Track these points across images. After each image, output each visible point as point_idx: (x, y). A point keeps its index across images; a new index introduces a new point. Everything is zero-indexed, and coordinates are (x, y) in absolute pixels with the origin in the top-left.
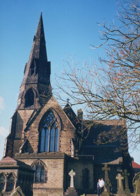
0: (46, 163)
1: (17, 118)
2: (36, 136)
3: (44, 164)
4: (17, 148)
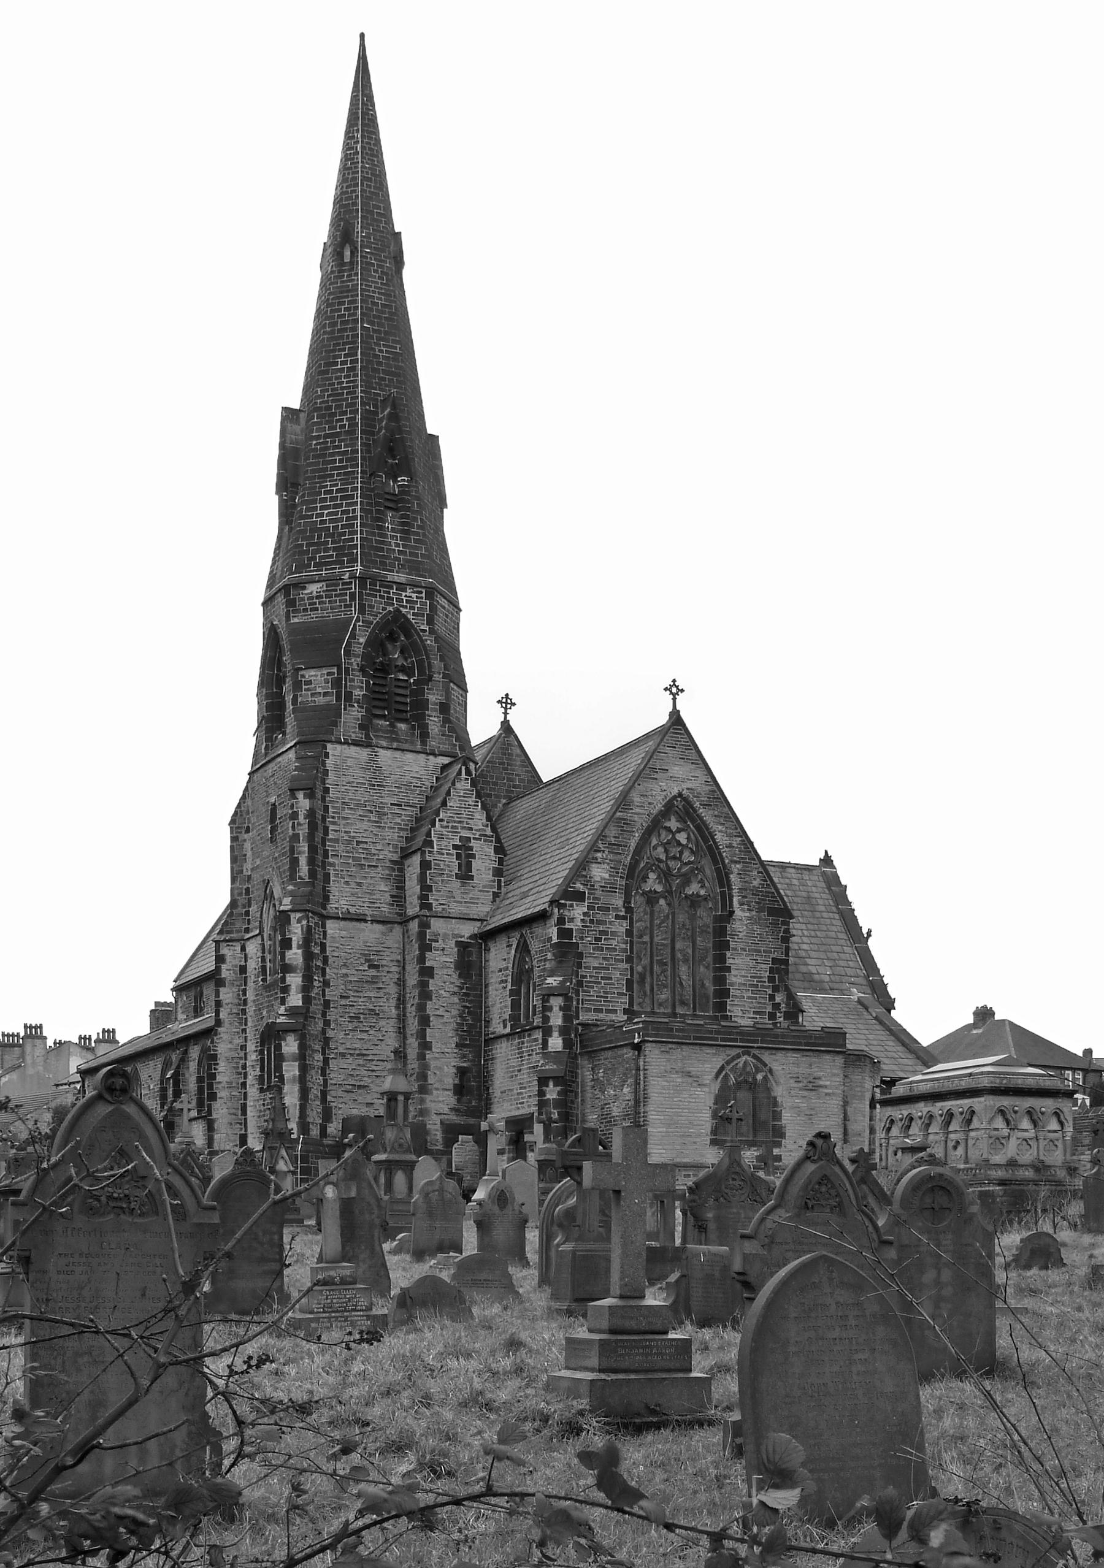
0: (776, 1067)
1: (327, 790)
2: (614, 933)
3: (771, 1071)
4: (345, 965)
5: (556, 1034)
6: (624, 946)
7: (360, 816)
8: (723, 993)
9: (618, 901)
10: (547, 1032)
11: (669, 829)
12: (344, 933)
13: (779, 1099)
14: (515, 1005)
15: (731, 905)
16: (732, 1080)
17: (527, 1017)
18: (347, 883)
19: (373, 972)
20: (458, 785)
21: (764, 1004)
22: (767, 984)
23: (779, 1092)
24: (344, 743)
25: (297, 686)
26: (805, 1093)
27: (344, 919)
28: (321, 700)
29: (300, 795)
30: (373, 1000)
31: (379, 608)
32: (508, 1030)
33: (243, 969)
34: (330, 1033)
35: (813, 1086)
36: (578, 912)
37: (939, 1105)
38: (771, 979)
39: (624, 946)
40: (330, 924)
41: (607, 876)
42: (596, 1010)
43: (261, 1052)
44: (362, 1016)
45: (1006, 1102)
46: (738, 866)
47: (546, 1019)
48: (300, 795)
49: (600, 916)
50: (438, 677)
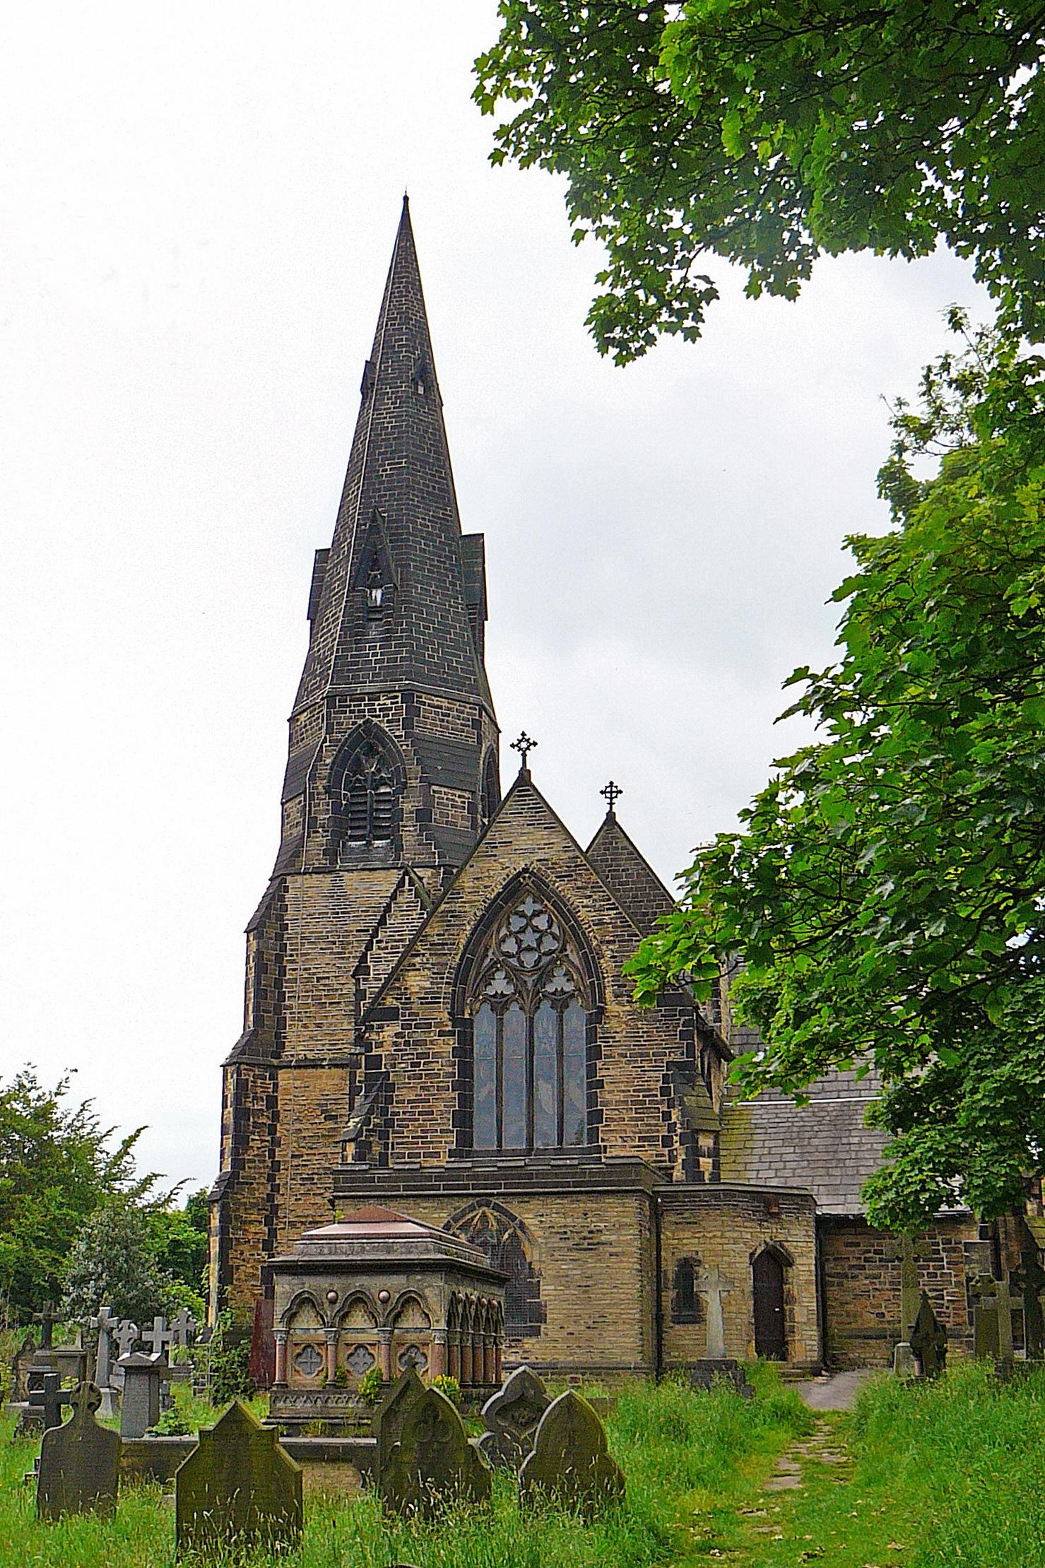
0: (530, 1221)
3: (522, 1226)
6: (450, 1070)
7: (322, 949)
11: (522, 915)
12: (298, 1083)
13: (536, 1266)
15: (602, 999)
18: (305, 1026)
20: (400, 899)
21: (656, 1125)
22: (659, 1098)
23: (532, 1255)
24: (305, 874)
26: (576, 1255)
27: (295, 1067)
30: (329, 1156)
31: (348, 722)
35: (590, 1243)
36: (391, 1030)
38: (665, 1091)
39: (450, 1070)
40: (282, 1074)
41: (428, 984)
44: (316, 1176)
46: (611, 947)
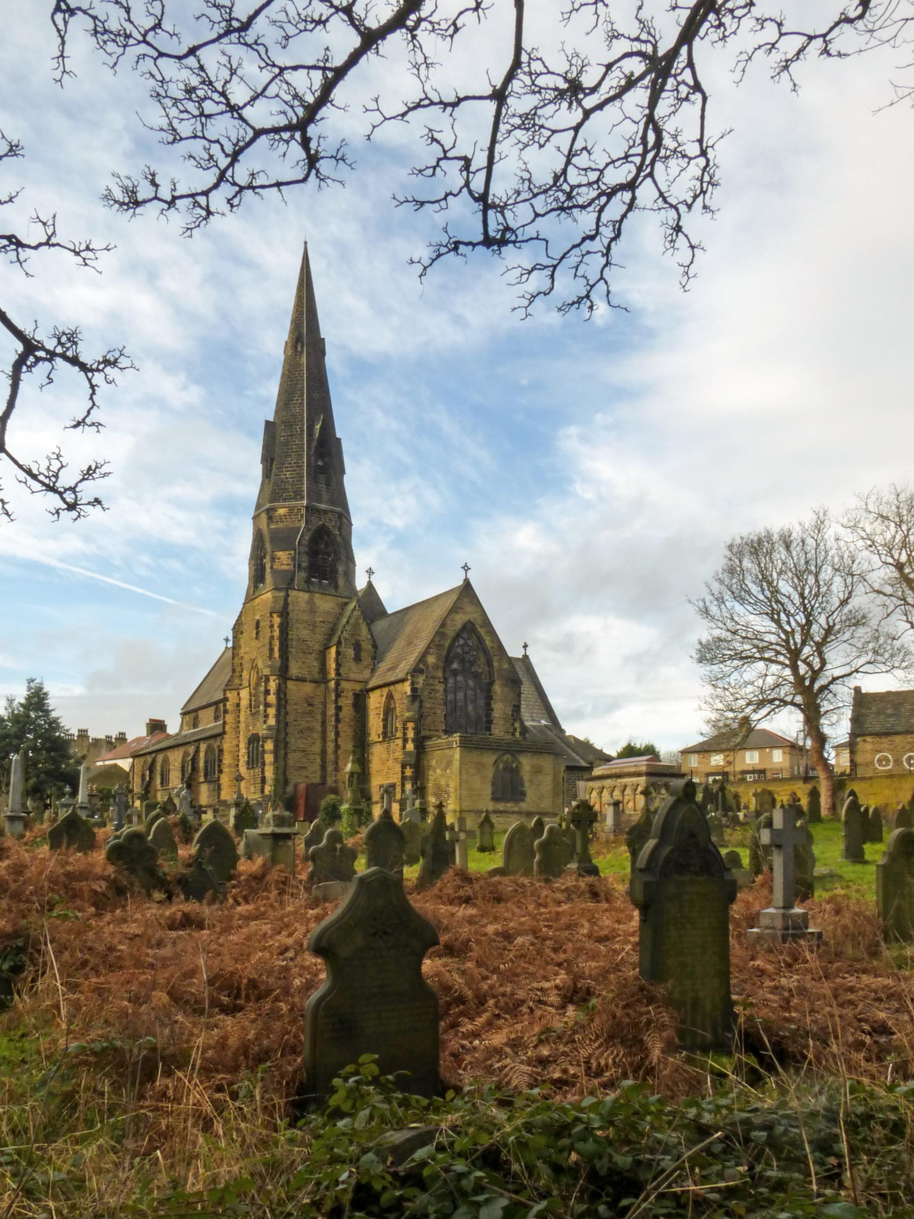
5: (410, 742)
8: (490, 722)
9: (440, 674)
10: (405, 740)
14: (385, 727)
16: (501, 766)
17: (392, 733)
19: (309, 708)
25: (273, 559)
28: (285, 567)
29: (275, 615)
31: (317, 523)
32: (381, 739)
33: (238, 705)
34: (288, 739)
36: (421, 679)
37: (619, 780)
38: (513, 715)
42: (430, 730)
43: (248, 748)
45: (655, 779)
47: (405, 734)
48: (275, 615)
49: (431, 681)
50: (343, 558)
